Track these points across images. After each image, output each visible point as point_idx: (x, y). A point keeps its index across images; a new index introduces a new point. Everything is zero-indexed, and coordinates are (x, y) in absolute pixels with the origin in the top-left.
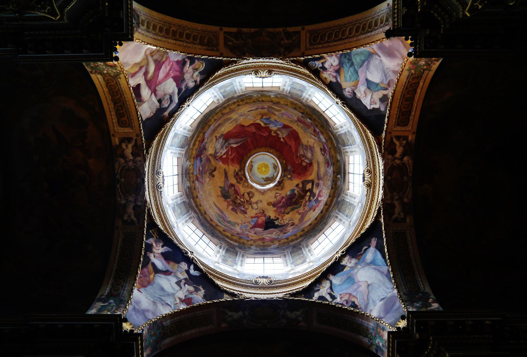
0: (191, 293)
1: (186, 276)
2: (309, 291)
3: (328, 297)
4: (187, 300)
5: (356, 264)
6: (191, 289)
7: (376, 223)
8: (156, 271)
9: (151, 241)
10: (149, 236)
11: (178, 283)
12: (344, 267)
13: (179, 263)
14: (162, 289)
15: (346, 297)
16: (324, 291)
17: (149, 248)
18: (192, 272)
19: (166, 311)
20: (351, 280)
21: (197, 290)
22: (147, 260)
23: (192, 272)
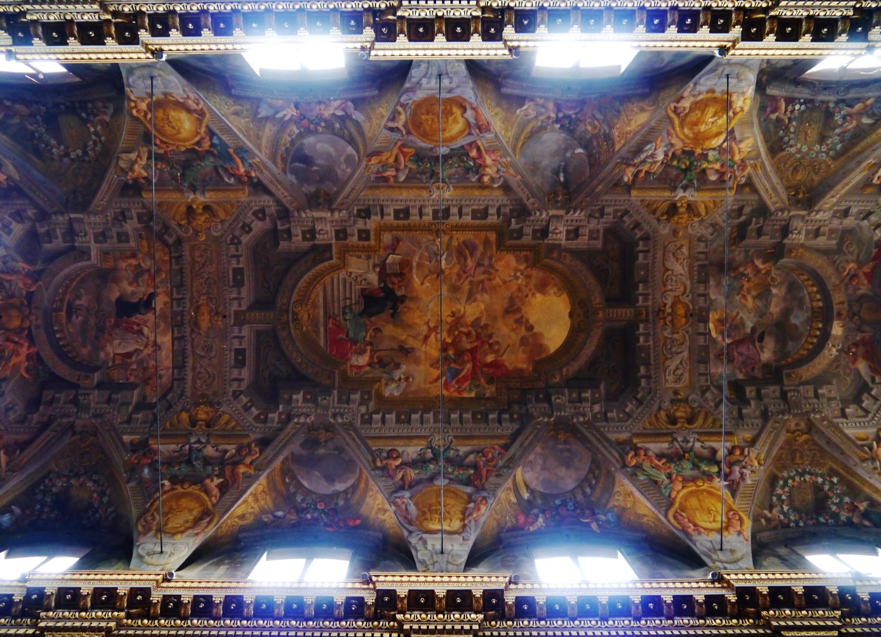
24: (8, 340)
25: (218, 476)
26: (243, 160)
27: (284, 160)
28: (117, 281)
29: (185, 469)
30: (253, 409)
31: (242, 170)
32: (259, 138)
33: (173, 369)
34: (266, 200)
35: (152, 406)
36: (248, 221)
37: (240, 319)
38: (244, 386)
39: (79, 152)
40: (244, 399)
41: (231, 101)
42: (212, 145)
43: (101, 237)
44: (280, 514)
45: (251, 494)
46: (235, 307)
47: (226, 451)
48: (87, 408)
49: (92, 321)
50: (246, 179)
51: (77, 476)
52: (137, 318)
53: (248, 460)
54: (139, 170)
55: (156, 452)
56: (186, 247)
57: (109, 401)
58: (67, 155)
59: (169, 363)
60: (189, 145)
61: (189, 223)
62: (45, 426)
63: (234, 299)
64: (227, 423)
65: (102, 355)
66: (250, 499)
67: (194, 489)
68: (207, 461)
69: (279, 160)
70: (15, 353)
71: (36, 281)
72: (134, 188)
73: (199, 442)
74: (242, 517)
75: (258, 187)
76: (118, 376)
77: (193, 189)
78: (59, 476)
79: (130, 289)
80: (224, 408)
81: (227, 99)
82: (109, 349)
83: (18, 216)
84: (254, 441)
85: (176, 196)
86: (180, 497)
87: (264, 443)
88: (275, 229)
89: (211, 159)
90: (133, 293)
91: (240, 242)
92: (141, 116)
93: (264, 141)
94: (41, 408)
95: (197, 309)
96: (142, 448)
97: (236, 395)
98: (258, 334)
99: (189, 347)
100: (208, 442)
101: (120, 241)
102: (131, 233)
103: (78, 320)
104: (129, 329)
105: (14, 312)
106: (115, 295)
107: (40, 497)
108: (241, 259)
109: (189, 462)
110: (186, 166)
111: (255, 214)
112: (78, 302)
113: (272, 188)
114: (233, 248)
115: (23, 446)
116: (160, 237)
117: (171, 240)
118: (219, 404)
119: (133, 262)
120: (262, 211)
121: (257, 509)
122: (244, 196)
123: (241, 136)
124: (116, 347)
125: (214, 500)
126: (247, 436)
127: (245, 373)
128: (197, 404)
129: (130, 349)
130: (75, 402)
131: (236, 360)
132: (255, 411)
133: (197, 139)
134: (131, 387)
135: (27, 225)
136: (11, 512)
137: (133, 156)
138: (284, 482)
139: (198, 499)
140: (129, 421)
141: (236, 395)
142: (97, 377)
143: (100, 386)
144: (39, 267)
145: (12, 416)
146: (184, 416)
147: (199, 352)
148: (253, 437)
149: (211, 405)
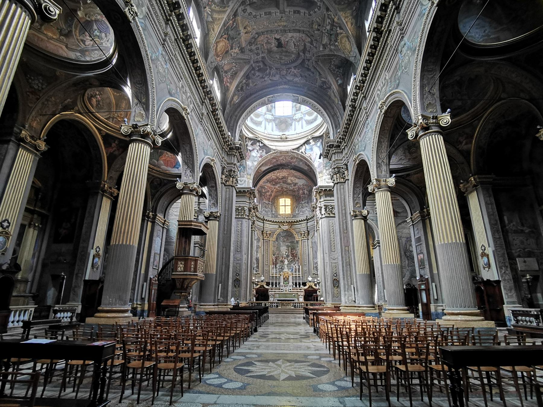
0: (261, 153)
1: (259, 147)
2: (298, 148)
3: (304, 153)
4: (261, 156)
5: (314, 144)
6: (261, 151)
7: (322, 136)
8: (250, 151)
9: (247, 143)
10: (246, 141)
11: (257, 151)
12: (310, 143)
13: (256, 144)
14: (253, 156)
15: (309, 155)
16: (303, 149)
17: (247, 145)
18: (261, 145)
19: (256, 163)
20: (311, 149)
21: (263, 151)
22: (247, 149)
23: (261, 145)
24: (290, 73)
25: (337, 28)
26: (228, 23)
27: (224, 8)
28: (271, 48)
29: (333, 36)
30: (315, 10)
31: (231, 22)
32: (219, 19)
33: (299, 33)
34: (240, 10)
35: (312, 41)
36: (248, 14)
37: (283, 12)
38: (307, 12)
39: (234, 64)
40: (311, 13)
41: (210, 33)
42: (225, 34)
43: (258, 54)
44: (354, 8)
45: (345, 19)
46: (279, 14)
47: (329, 23)
48: (310, 57)
49: (284, 54)
50: (233, 20)
51: (331, 62)
52: (283, 42)
53: (333, 17)
54: (237, 50)
55: (326, 43)
56: (259, 31)
57: (309, 52)
58: (235, 66)
59: (298, 34)
60: (226, 41)
61: (250, 32)
62: (315, 68)
63: (275, 14)
64: (320, 20)
65: (295, 52)
66: (346, 20)
67: (340, 37)
68: (332, 30)
69: (225, 9)
70: (294, 72)
71: (272, 68)
72: (242, 50)
73: (325, 30)
74: (352, 24)
75: (235, 15)
76: (302, 48)
77: (239, 34)
78: (330, 67)
79: (273, 45)
80: (314, 19)
81: (210, 35)
82: (293, 50)
83: (254, 75)
84: (326, 12)
85: (242, 38)
86: (341, 40)
87: (328, 9)
88: (249, 4)
89: (229, 32)
90: (275, 44)
91: (255, 15)
92: (221, 57)
93: (220, 17)
94: (310, 68)
95: (279, 26)
96: (324, 46)
97: (310, 15)
98: (288, 6)
99: (293, 28)
100: (325, 27)
101: (259, 49)
102: (255, 47)
103: (284, 58)
104: (287, 45)
105: (282, 72)
106: (275, 49)
107: (335, 72)
108: (261, 13)
109: (331, 35)
110: (233, 39)
111: (245, 13)
112: (278, 58)
113: (235, 11)
114: (257, 17)
115: (320, 74)
116: (256, 39)
117: (257, 36)
118: (313, 21)
119: (265, 45)
120: (243, 11)
121: (350, 17)
122: (239, 18)
123: (220, 27)
124: (292, 48)
125: (344, 33)
126: (325, 14)
127: (302, 11)
128: (312, 28)
129: (293, 44)
130: (309, 60)
131: (298, 13)
132: (316, 10)
133: (224, 40)
134: (305, 45)
135: (256, 72)
136: (338, 80)
137: (232, 54)
138: (343, 5)
139: (343, 37)
140: (316, 48)
141: (310, 15)
142: (301, 54)
143: (304, 53)
144: (268, 67)
145: (312, 75)
146: (316, 32)
147: (294, 25)
148: (325, 12)
149: (313, 23)
